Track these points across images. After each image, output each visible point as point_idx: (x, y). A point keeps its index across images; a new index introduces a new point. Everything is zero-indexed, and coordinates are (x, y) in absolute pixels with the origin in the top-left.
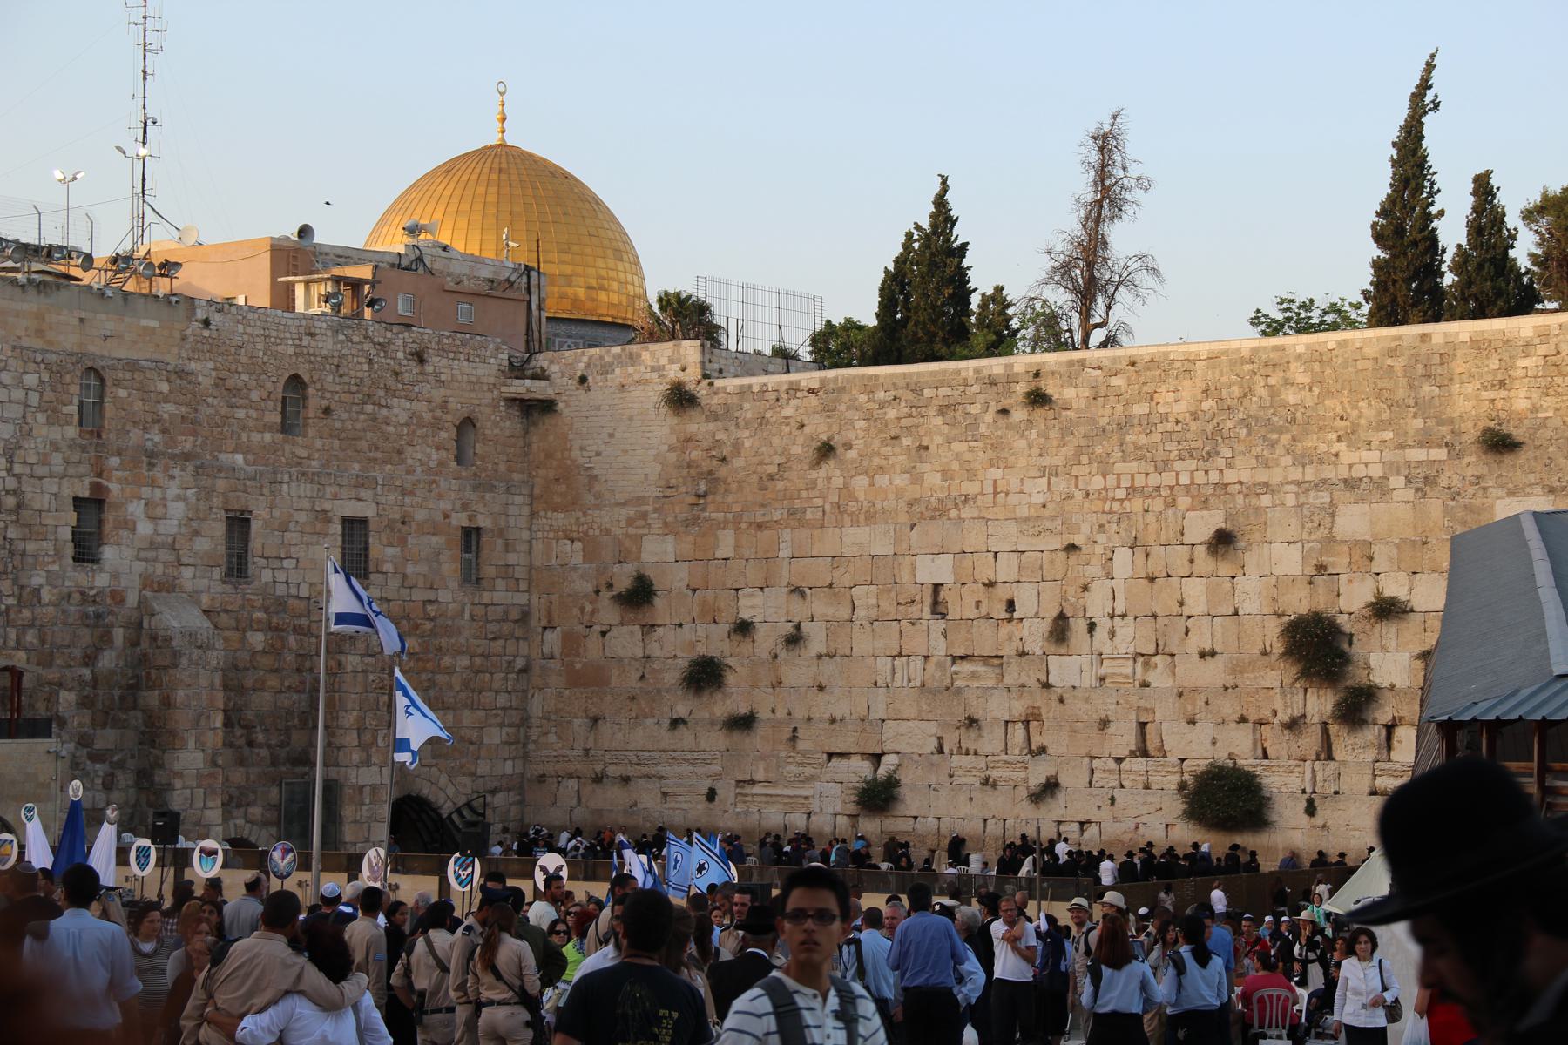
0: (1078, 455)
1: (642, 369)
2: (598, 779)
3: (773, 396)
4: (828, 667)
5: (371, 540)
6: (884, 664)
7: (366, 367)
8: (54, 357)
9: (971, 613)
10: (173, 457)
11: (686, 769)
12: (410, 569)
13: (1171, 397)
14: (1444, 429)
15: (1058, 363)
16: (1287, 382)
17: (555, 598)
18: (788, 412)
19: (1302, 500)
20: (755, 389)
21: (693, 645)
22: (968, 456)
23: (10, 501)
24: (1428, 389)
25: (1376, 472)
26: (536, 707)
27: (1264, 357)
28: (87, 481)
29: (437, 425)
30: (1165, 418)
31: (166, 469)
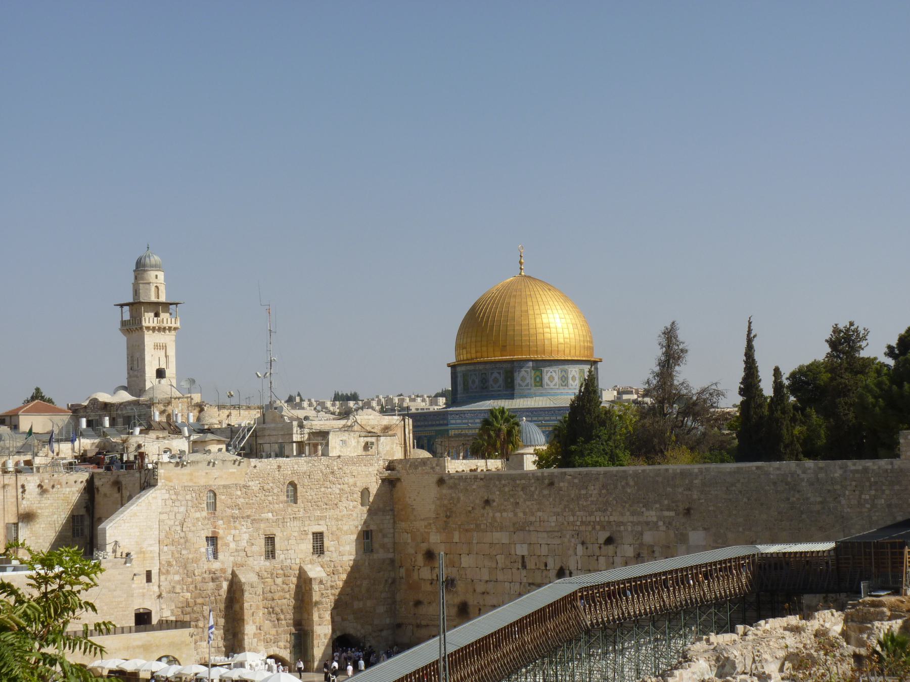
0: (565, 508)
1: (428, 468)
4: (491, 585)
7: (321, 475)
9: (533, 567)
12: (342, 549)
14: (674, 505)
16: (627, 484)
18: (474, 487)
23: (182, 541)
24: (669, 489)
25: (655, 519)
26: (398, 597)
27: (620, 474)
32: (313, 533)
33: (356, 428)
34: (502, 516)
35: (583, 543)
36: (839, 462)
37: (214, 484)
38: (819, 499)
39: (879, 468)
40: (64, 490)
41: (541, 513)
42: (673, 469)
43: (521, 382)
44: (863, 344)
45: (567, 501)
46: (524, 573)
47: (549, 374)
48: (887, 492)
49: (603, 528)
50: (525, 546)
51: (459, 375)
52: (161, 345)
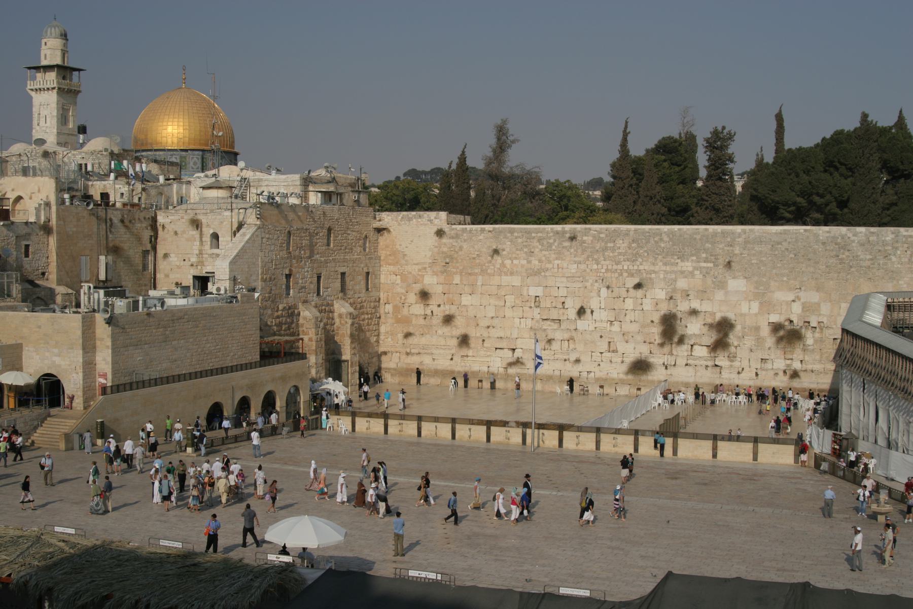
2: (408, 354)
4: (496, 322)
6: (517, 321)
11: (442, 351)
14: (712, 257)
15: (581, 228)
16: (661, 240)
18: (481, 237)
19: (666, 276)
20: (468, 229)
21: (444, 311)
24: (708, 245)
25: (690, 269)
27: (653, 232)
28: (288, 268)
30: (619, 248)
32: (343, 274)
34: (512, 263)
35: (608, 287)
36: (892, 229)
38: (871, 257)
41: (560, 261)
42: (713, 229)
43: (193, 166)
45: (591, 252)
46: (538, 310)
49: (631, 275)
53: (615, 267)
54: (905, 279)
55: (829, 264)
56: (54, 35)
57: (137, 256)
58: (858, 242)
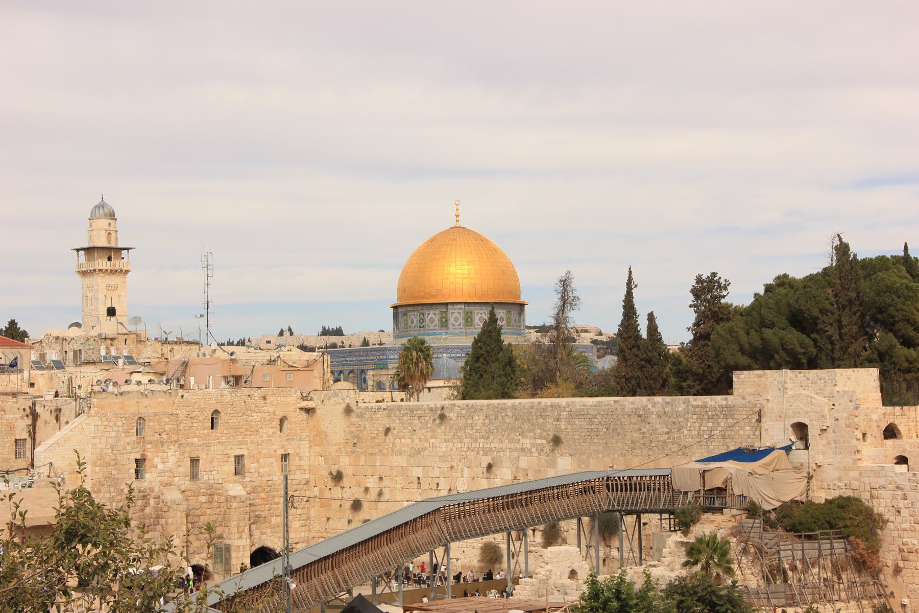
0: (454, 435)
3: (373, 410)
5: (246, 462)
7: (243, 404)
8: (127, 415)
10: (171, 442)
12: (261, 470)
13: (477, 418)
14: (545, 434)
17: (316, 476)
22: (426, 434)
23: (113, 463)
24: (541, 420)
25: (529, 446)
28: (139, 453)
29: (272, 420)
30: (476, 425)
31: (168, 446)
32: (236, 456)
33: (279, 363)
37: (143, 412)
38: (666, 430)
39: (716, 403)
40: (7, 416)
42: (545, 403)
43: (454, 323)
44: (724, 293)
47: (480, 315)
48: (722, 424)
49: (486, 454)
50: (421, 468)
51: (400, 315)
52: (113, 286)
53: (474, 445)
54: (697, 454)
55: (633, 439)
56: (98, 215)
57: (7, 445)
58: (657, 414)
